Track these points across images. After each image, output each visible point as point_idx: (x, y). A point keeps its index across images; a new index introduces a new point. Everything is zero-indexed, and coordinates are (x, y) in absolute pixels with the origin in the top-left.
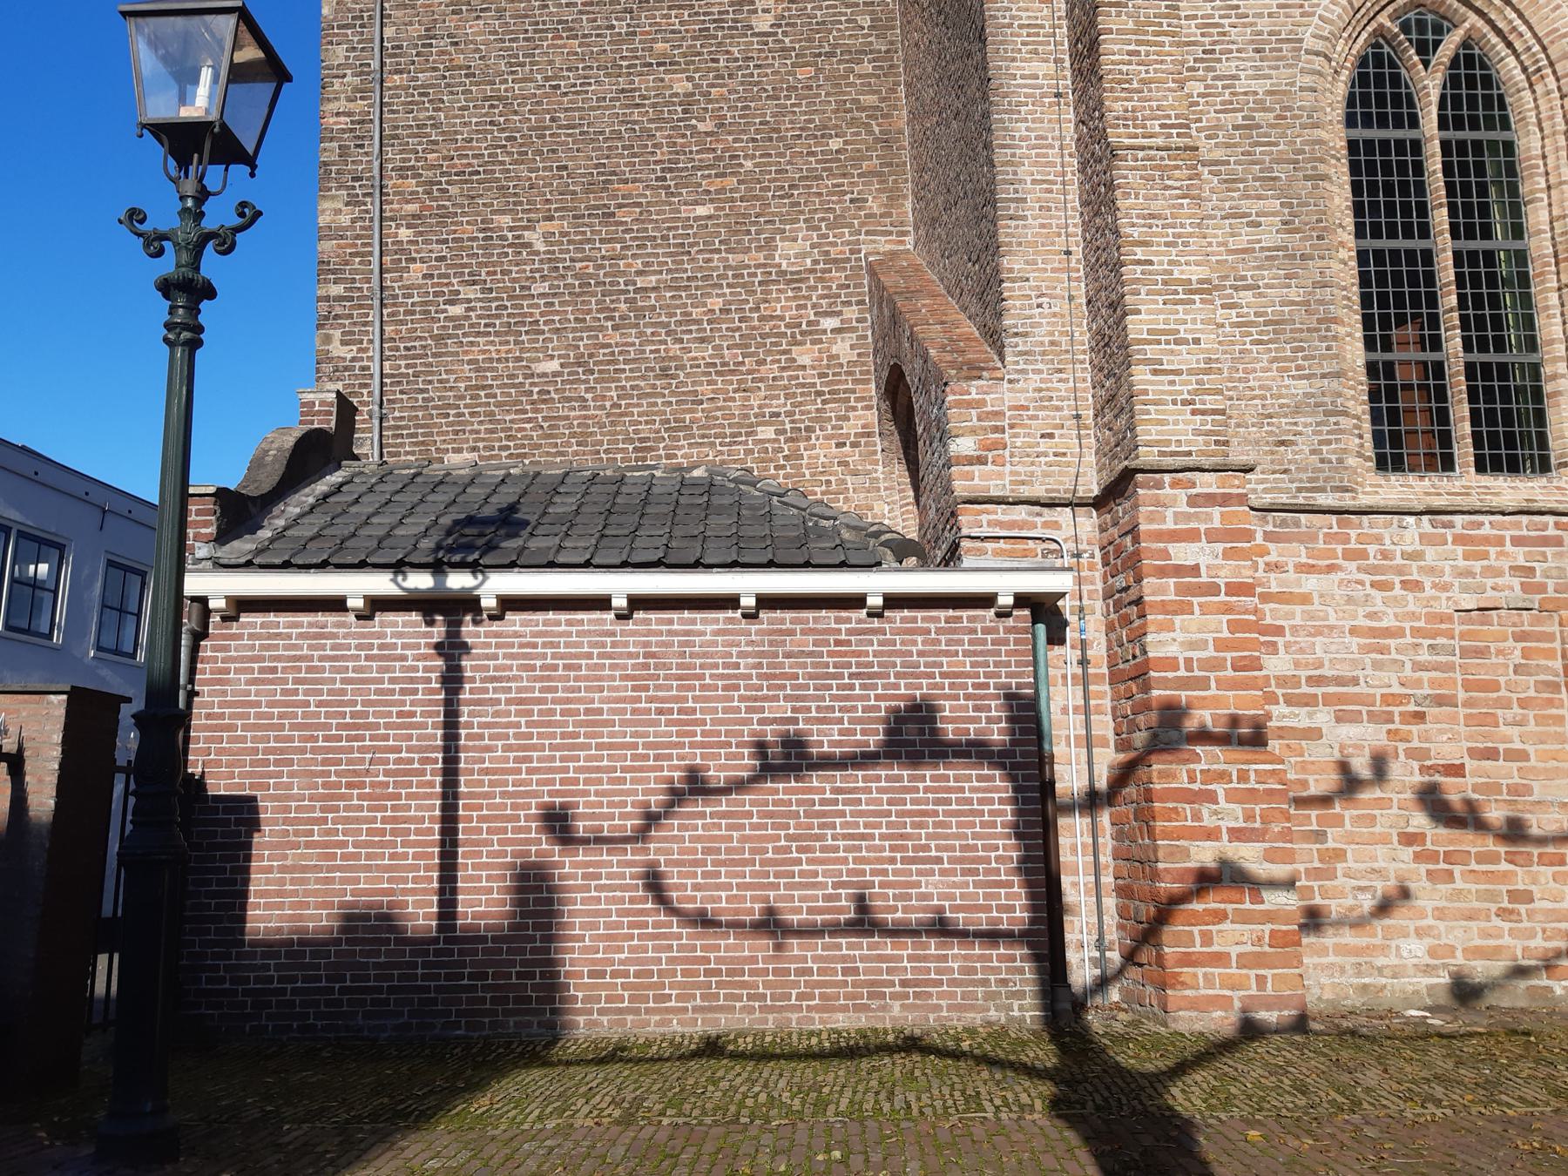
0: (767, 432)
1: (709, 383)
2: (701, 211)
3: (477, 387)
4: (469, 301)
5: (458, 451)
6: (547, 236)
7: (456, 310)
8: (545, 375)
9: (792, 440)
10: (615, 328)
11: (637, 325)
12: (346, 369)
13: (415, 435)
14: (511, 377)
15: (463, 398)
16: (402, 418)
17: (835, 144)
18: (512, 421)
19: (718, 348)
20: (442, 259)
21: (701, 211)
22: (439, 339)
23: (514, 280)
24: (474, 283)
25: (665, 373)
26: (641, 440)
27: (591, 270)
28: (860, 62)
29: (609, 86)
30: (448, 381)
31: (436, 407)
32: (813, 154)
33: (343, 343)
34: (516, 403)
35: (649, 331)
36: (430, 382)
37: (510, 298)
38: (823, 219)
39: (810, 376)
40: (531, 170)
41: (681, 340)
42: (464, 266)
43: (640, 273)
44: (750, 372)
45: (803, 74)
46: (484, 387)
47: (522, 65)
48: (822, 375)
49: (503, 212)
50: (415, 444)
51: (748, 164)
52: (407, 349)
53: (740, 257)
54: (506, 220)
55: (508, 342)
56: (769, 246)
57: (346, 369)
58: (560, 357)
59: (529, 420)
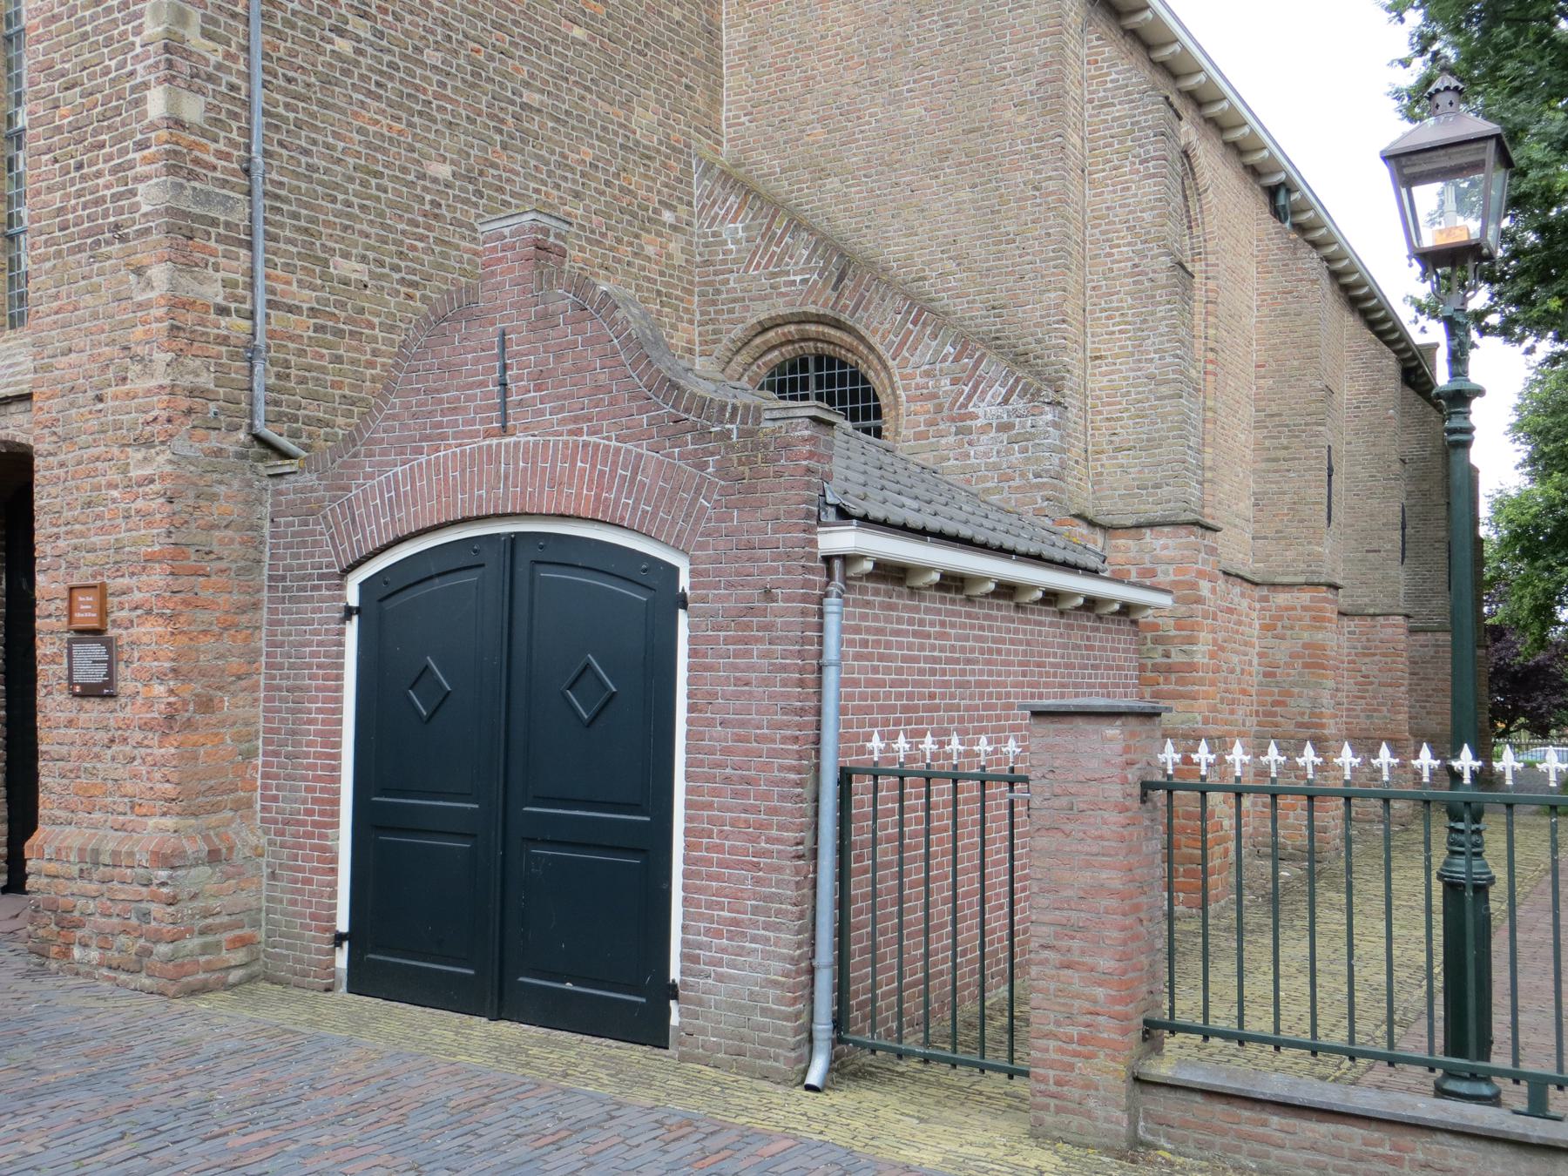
1: (582, 249)
2: (578, 32)
4: (358, 40)
5: (346, 255)
7: (344, 46)
8: (435, 180)
11: (521, 152)
12: (210, 78)
13: (296, 216)
15: (351, 179)
16: (281, 184)
18: (403, 232)
19: (586, 208)
21: (578, 32)
23: (407, 33)
27: (481, 57)
30: (333, 148)
31: (321, 183)
33: (206, 34)
34: (409, 209)
35: (533, 163)
36: (315, 142)
38: (667, 96)
39: (653, 271)
41: (558, 187)
44: (611, 249)
48: (662, 274)
50: (298, 229)
52: (289, 80)
53: (607, 107)
55: (398, 119)
56: (626, 104)
57: (210, 78)
58: (453, 162)
59: (422, 238)
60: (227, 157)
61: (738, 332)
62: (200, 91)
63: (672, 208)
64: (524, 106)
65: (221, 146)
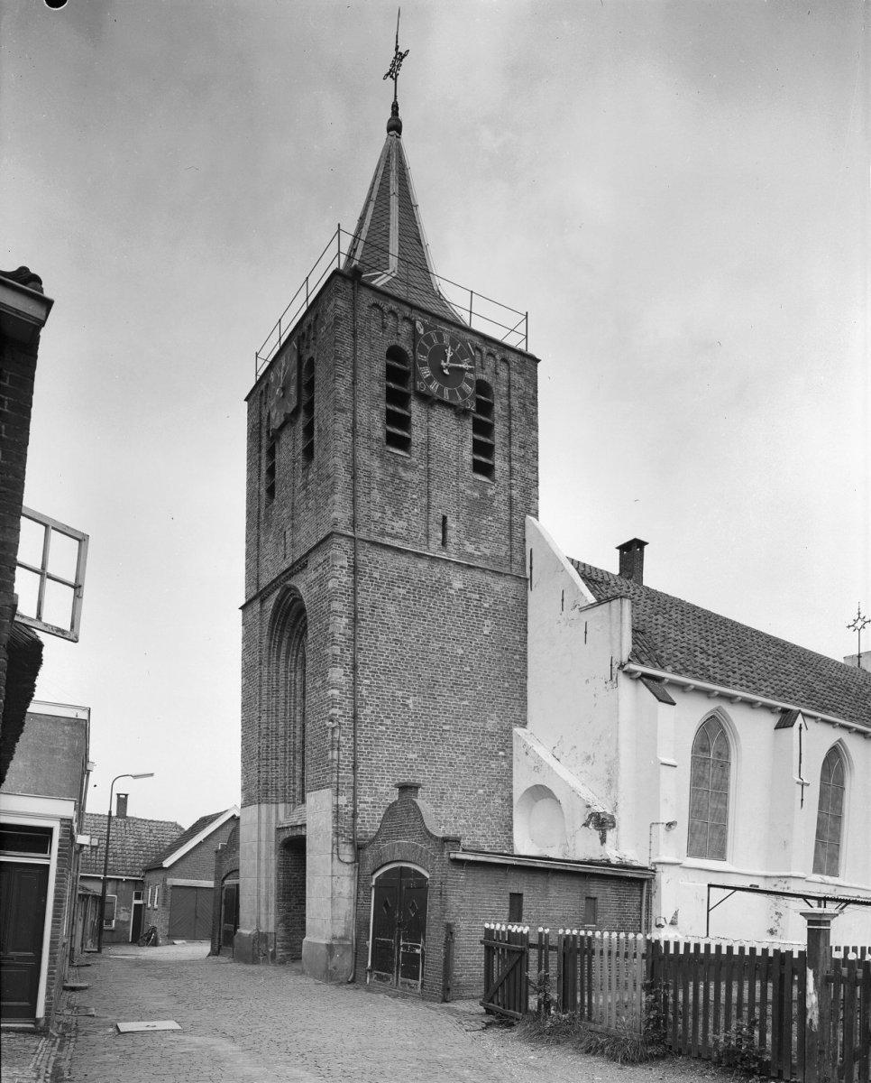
0: (481, 791)
2: (466, 703)
3: (390, 761)
6: (414, 702)
7: (384, 728)
9: (488, 795)
10: (436, 744)
13: (367, 777)
17: (506, 685)
24: (389, 718)
25: (451, 765)
29: (437, 645)
32: (499, 687)
34: (403, 769)
37: (401, 726)
40: (409, 674)
42: (386, 710)
43: (444, 724)
45: (498, 655)
46: (392, 761)
47: (407, 628)
49: (399, 690)
51: (480, 688)
53: (476, 723)
54: (400, 693)
56: (484, 721)
60: (348, 766)
63: (504, 750)
65: (347, 763)
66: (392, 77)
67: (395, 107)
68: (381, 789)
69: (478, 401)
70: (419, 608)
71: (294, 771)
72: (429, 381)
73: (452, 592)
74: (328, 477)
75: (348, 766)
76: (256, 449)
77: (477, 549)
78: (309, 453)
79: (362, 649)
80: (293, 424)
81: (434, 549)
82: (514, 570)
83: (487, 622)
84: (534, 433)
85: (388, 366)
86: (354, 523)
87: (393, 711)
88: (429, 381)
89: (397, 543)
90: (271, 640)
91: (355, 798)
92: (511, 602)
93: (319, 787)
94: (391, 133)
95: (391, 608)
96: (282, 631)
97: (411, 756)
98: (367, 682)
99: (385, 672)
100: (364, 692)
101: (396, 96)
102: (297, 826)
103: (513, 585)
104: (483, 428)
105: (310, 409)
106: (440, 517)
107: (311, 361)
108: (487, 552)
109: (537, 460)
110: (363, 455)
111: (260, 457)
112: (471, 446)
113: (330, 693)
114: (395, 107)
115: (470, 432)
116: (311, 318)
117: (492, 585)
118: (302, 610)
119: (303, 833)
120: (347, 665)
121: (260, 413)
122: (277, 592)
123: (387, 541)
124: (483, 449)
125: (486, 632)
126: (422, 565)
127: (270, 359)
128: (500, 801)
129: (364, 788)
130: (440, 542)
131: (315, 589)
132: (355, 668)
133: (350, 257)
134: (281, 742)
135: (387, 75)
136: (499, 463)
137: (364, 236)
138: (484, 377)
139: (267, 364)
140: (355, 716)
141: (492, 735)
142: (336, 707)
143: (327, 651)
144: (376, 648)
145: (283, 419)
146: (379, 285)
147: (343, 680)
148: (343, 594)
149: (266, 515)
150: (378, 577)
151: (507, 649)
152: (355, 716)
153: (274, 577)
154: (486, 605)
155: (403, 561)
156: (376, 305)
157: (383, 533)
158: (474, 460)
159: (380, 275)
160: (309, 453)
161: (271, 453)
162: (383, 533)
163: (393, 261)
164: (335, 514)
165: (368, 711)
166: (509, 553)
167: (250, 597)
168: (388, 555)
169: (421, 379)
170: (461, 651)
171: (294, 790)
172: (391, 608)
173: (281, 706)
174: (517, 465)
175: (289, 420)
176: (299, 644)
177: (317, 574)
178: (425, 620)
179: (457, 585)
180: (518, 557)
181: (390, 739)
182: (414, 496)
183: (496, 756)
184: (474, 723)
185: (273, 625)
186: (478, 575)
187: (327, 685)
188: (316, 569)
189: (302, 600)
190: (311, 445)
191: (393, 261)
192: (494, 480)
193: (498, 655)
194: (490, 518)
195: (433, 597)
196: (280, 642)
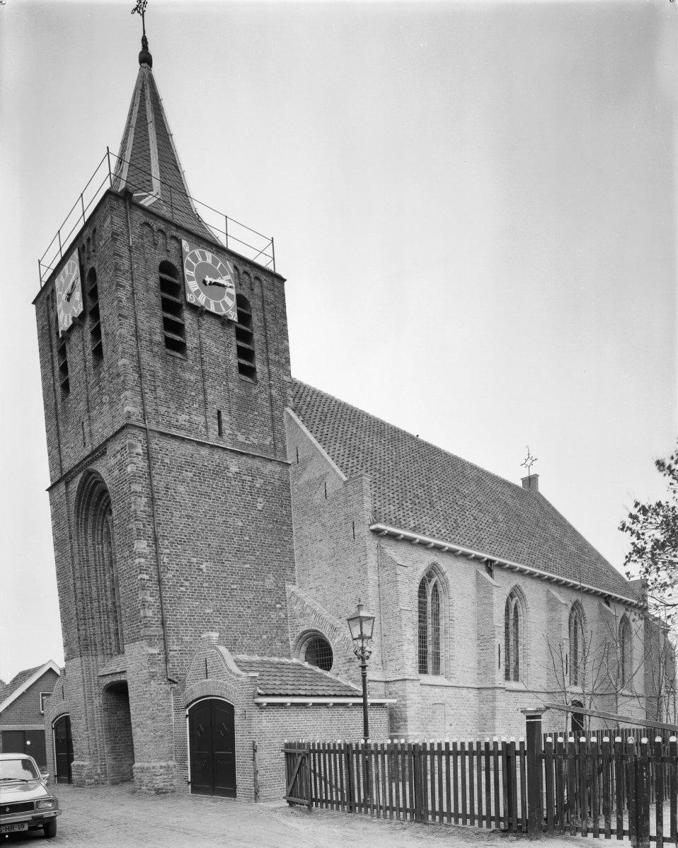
0: (265, 637)
2: (246, 566)
3: (190, 616)
6: (207, 567)
8: (208, 614)
13: (174, 630)
14: (200, 613)
17: (278, 550)
20: (177, 571)
22: (179, 598)
24: (188, 580)
25: (240, 616)
26: (235, 637)
28: (283, 526)
37: (198, 587)
43: (232, 584)
45: (271, 526)
46: (193, 616)
49: (194, 557)
54: (194, 560)
56: (263, 580)
60: (158, 621)
61: (298, 634)
62: (151, 609)
64: (231, 589)
66: (139, 12)
67: (144, 41)
68: (186, 639)
69: (239, 313)
70: (204, 488)
71: (109, 628)
72: (197, 293)
73: (230, 475)
74: (118, 375)
75: (158, 621)
76: (48, 349)
77: (247, 438)
78: (98, 352)
79: (160, 524)
80: (81, 326)
81: (212, 438)
82: (277, 457)
83: (260, 500)
84: (285, 342)
85: (161, 280)
86: (144, 416)
87: (190, 574)
88: (197, 293)
89: (182, 434)
90: (78, 517)
91: (165, 646)
92: (277, 483)
93: (134, 640)
94: (143, 64)
95: (181, 489)
96: (87, 509)
97: (208, 611)
98: (168, 551)
99: (181, 542)
100: (166, 560)
101: (144, 31)
102: (116, 673)
103: (278, 469)
104: (244, 336)
105: (95, 313)
106: (215, 411)
107: (93, 270)
108: (255, 441)
109: (289, 365)
110: (146, 357)
111: (52, 356)
112: (236, 352)
113: (137, 561)
114: (144, 41)
115: (234, 339)
116: (88, 232)
117: (262, 469)
118: (105, 491)
119: (123, 679)
120: (149, 537)
121: (49, 317)
122: (81, 475)
123: (174, 432)
124: (245, 354)
125: (260, 508)
126: (205, 452)
127: (54, 266)
128: (280, 644)
129: (172, 638)
130: (216, 433)
131: (116, 472)
132: (156, 540)
133: (118, 178)
134: (95, 604)
135: (135, 9)
136: (259, 366)
137: (128, 158)
138: (242, 293)
139: (50, 272)
140: (159, 581)
141: (270, 591)
142: (143, 573)
143: (131, 526)
144: (172, 522)
145: (71, 322)
146: (147, 205)
147: (147, 551)
148: (140, 477)
149: (64, 408)
150: (169, 462)
151: (277, 521)
152: (159, 581)
153: (77, 462)
154: (258, 486)
155: (189, 449)
156: (147, 224)
157: (170, 425)
158: (239, 364)
159: (146, 196)
160: (98, 352)
161: (62, 352)
162: (170, 425)
163: (156, 184)
164: (126, 409)
165: (169, 576)
166: (273, 442)
167: (55, 480)
168: (176, 444)
169: (190, 293)
170: (240, 524)
171: (110, 644)
172: (181, 489)
173: (93, 574)
174: (274, 369)
175: (78, 322)
176: (103, 521)
177: (116, 460)
178: (210, 499)
179: (234, 469)
180: (280, 445)
181: (190, 598)
182: (193, 394)
183: (275, 607)
184: (256, 583)
185: (79, 504)
186: (250, 461)
187: (133, 555)
188: (115, 456)
189: (103, 482)
190: (100, 345)
191: (156, 184)
192: (257, 382)
193: (271, 526)
194: (256, 413)
195: (215, 480)
196: (86, 519)
